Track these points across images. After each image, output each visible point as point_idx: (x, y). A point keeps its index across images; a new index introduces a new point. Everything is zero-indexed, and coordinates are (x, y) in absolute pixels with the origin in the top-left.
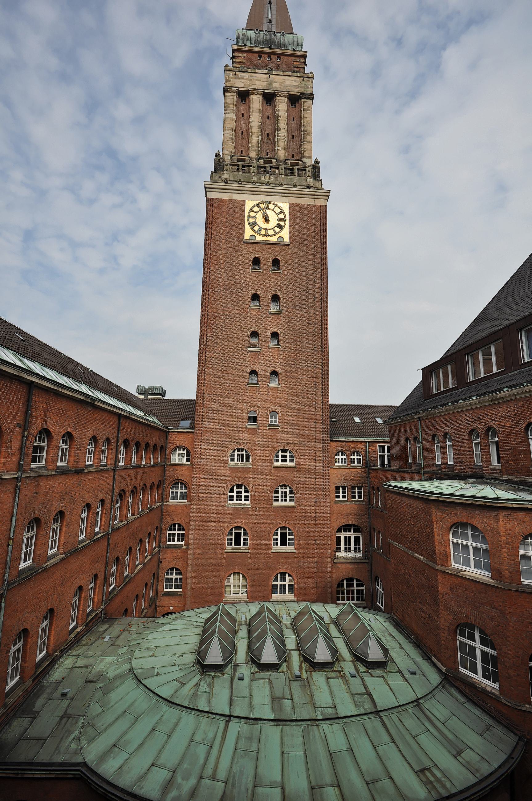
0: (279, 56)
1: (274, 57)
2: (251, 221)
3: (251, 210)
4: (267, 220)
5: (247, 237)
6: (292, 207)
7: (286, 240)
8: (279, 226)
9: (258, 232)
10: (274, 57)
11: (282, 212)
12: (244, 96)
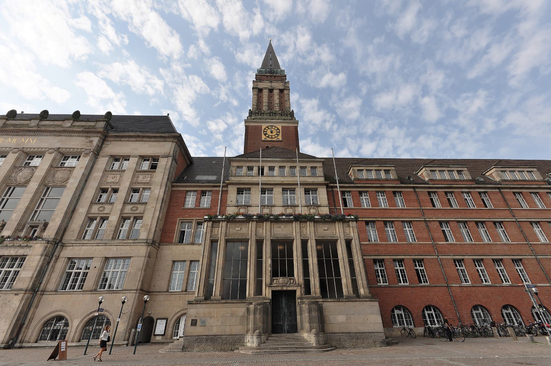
0: (275, 76)
1: (273, 77)
4: (272, 132)
5: (263, 139)
6: (282, 127)
7: (281, 139)
9: (268, 137)
10: (273, 77)
11: (278, 129)
12: (260, 90)
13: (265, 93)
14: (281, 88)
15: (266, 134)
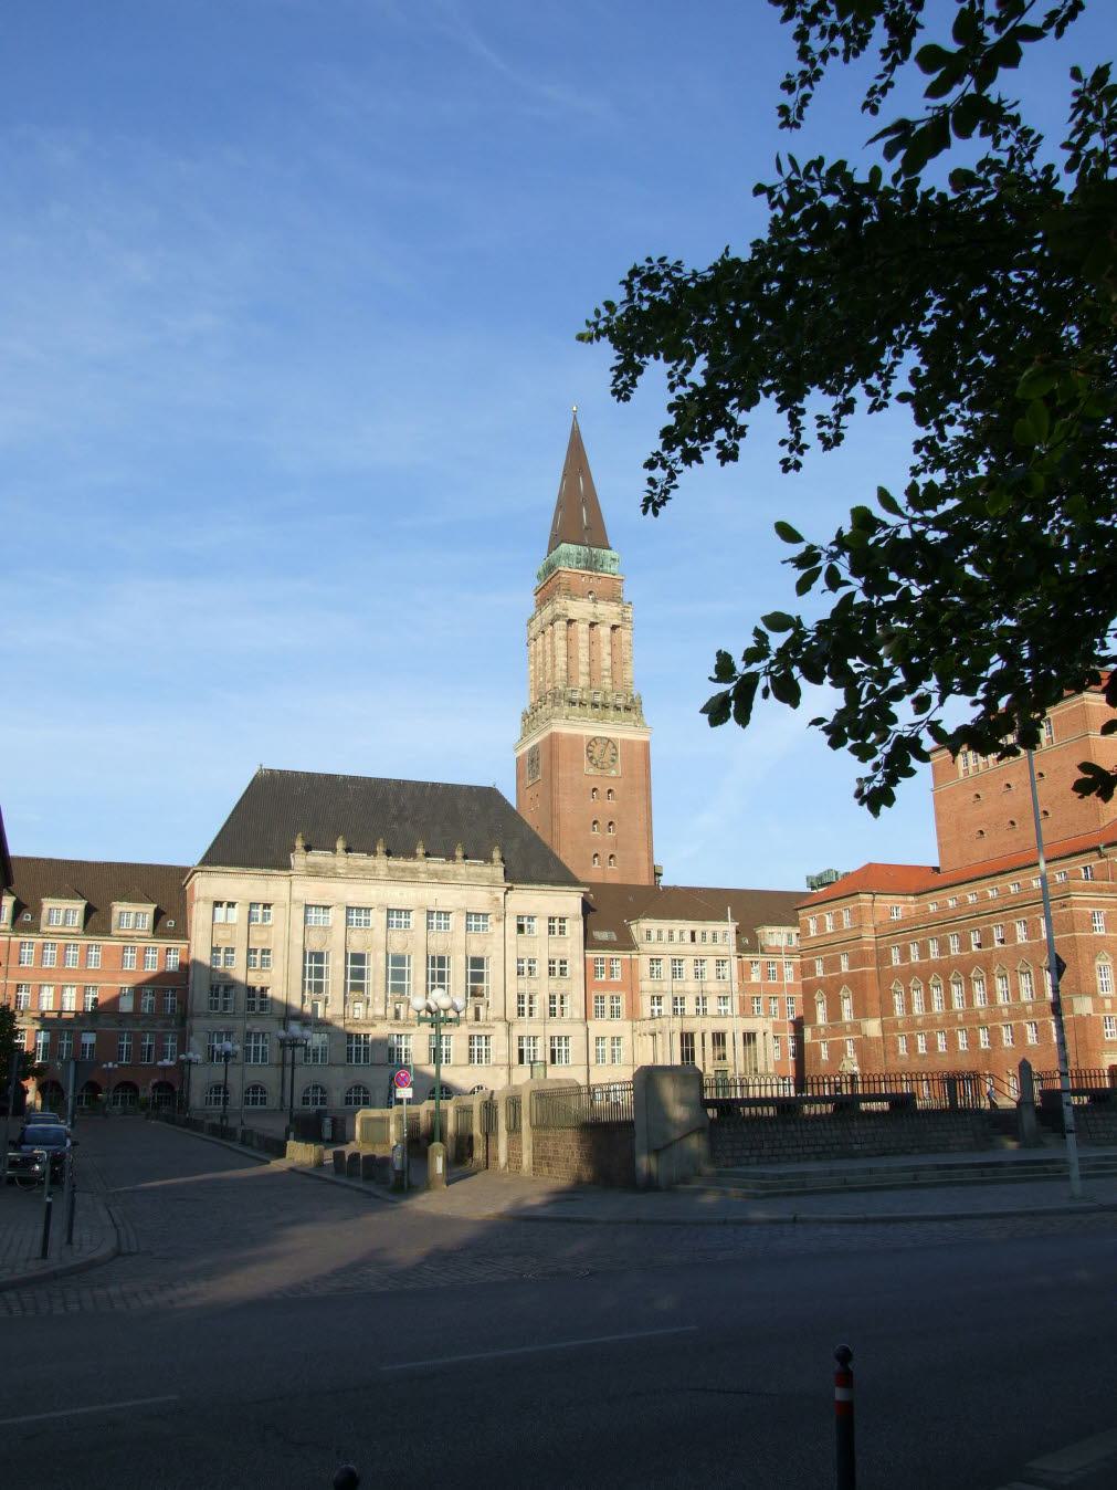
2: (590, 754)
11: (614, 747)
13: (583, 627)
14: (616, 622)
15: (592, 758)
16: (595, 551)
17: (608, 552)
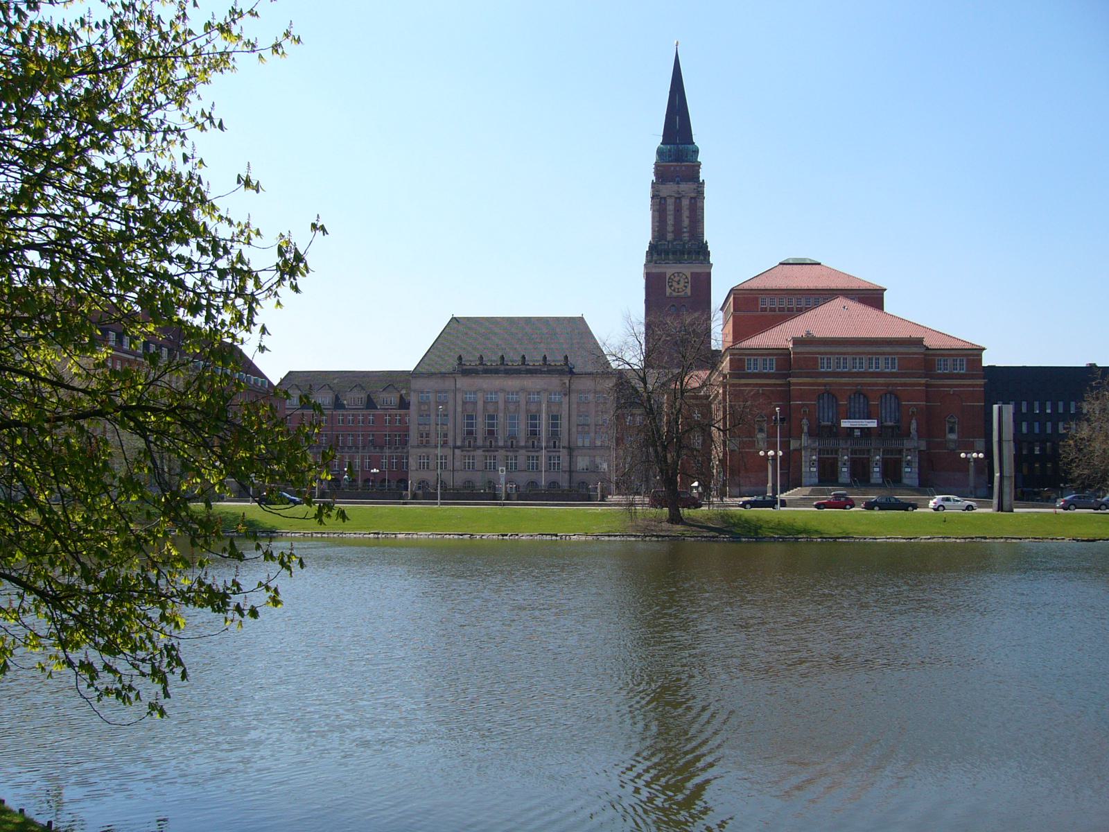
3: (670, 278)
5: (668, 294)
6: (692, 273)
8: (686, 287)
9: (674, 290)
13: (670, 202)
14: (693, 195)
15: (672, 286)
16: (681, 147)
17: (690, 147)
